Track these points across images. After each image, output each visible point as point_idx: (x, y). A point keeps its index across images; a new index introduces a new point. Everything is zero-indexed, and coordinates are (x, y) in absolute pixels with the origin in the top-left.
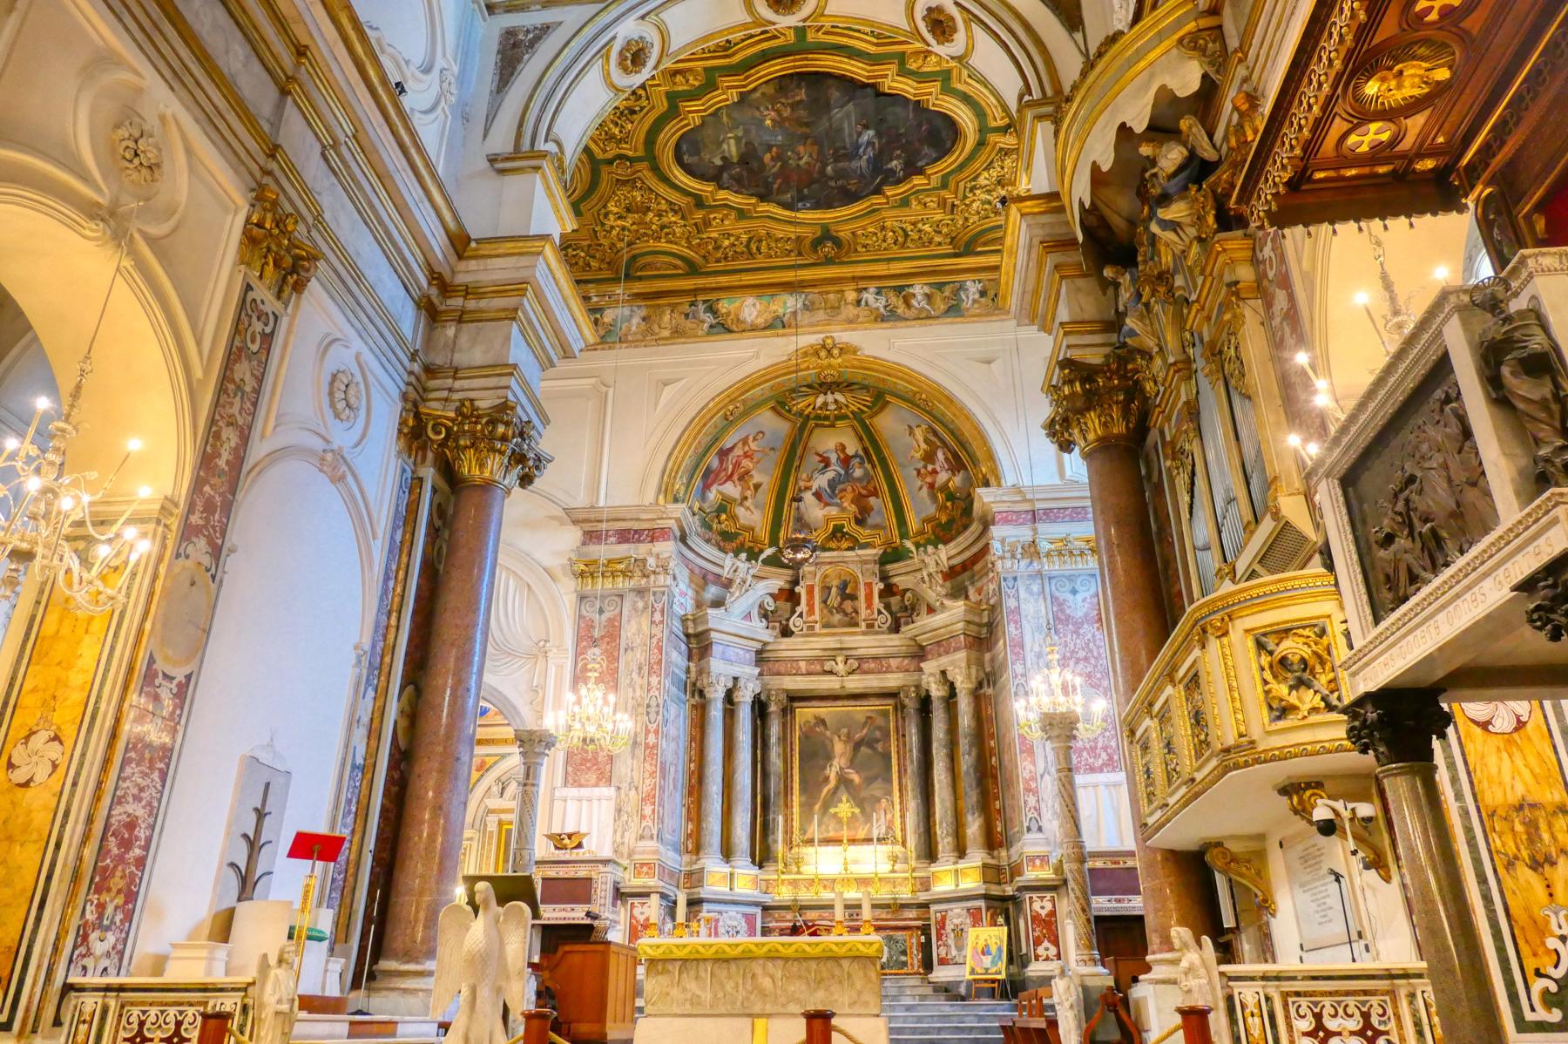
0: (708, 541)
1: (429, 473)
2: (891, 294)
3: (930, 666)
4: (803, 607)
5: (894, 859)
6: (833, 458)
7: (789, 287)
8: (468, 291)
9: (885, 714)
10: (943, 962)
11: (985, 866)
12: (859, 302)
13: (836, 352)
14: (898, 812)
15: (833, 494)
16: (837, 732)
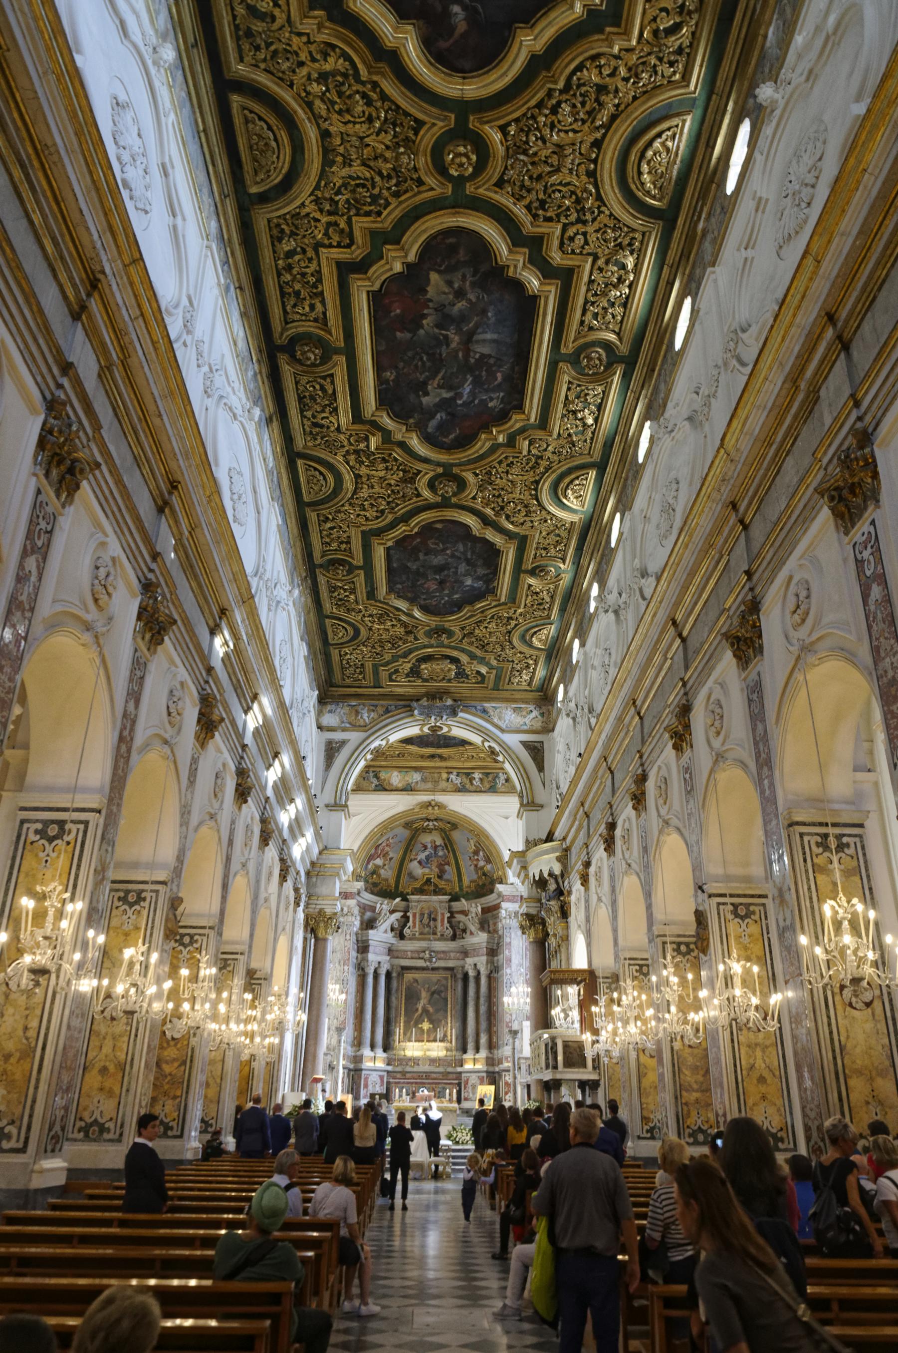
0: (366, 890)
3: (470, 961)
4: (410, 924)
5: (447, 1050)
6: (429, 846)
7: (416, 769)
9: (446, 978)
10: (466, 1099)
11: (487, 1058)
14: (451, 1029)
15: (427, 862)
16: (423, 986)
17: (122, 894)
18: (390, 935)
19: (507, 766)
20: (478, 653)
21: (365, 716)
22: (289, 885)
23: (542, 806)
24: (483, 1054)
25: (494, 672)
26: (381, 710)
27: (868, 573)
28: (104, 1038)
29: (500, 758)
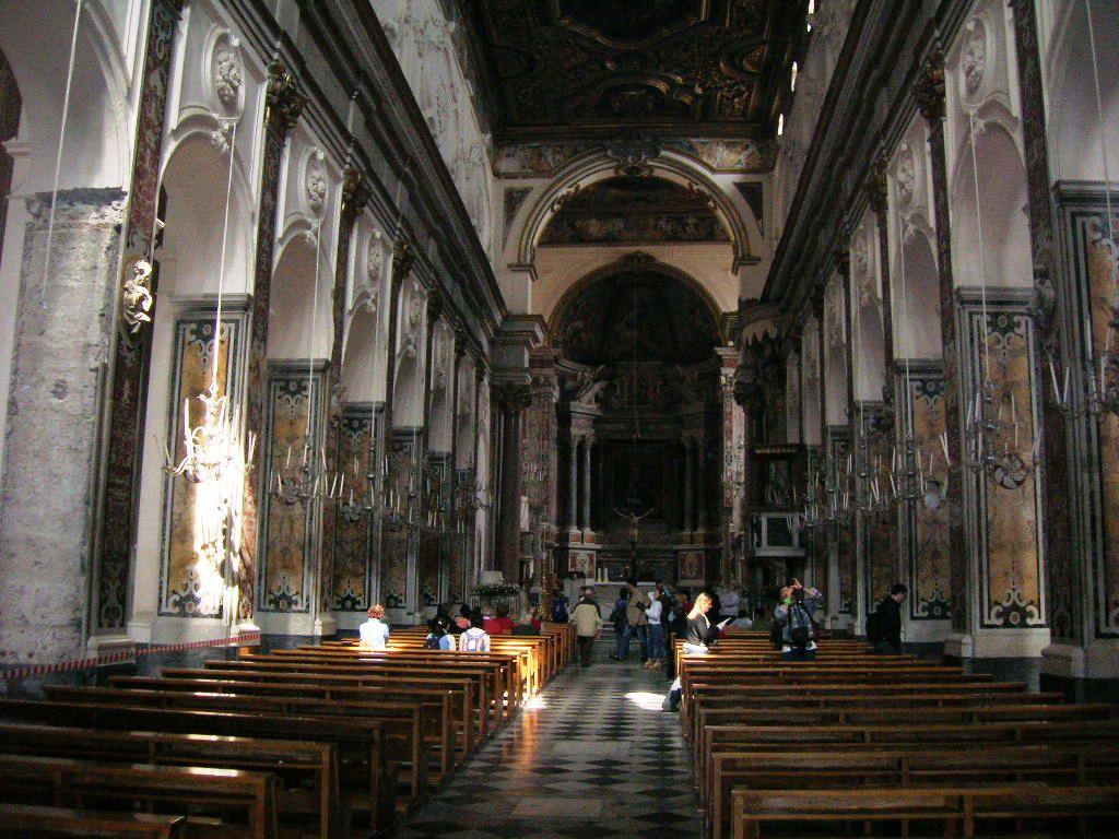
0: (565, 357)
1: (496, 411)
2: (675, 222)
3: (686, 434)
4: (618, 392)
7: (618, 215)
8: (506, 334)
10: (683, 578)
12: (656, 226)
13: (643, 260)
17: (282, 384)
18: (594, 406)
19: (719, 213)
20: (679, 79)
21: (550, 159)
22: (469, 358)
23: (759, 260)
24: (701, 531)
25: (700, 101)
26: (567, 151)
27: (1026, 44)
28: (282, 521)
29: (711, 204)
